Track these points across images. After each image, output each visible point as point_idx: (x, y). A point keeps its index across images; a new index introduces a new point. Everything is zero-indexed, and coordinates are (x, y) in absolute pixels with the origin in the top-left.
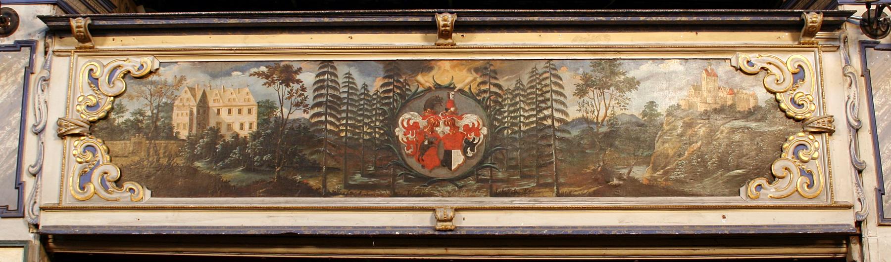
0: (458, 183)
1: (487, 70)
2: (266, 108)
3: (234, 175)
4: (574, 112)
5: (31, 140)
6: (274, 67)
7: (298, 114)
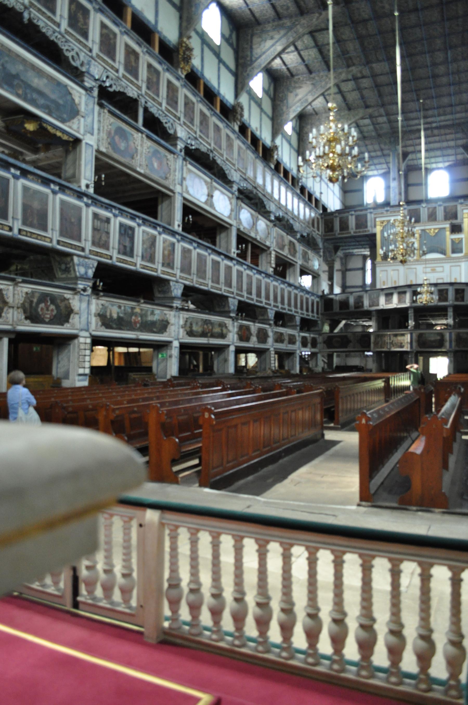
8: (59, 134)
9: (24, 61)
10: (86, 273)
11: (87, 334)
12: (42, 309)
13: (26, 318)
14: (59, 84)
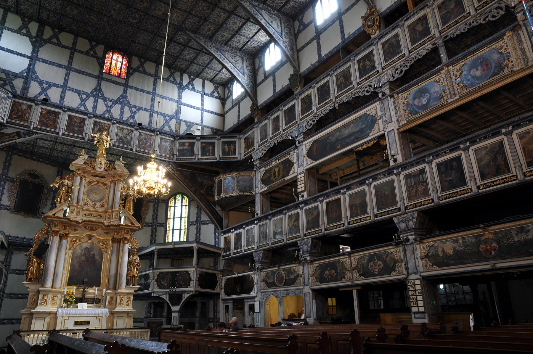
0: (494, 258)
1: (495, 234)
2: (454, 248)
3: (452, 262)
4: (516, 240)
5: (416, 260)
6: (454, 240)
7: (460, 249)
8: (365, 146)
9: (335, 130)
10: (407, 226)
11: (418, 276)
12: (371, 266)
13: (360, 275)
14: (360, 117)
